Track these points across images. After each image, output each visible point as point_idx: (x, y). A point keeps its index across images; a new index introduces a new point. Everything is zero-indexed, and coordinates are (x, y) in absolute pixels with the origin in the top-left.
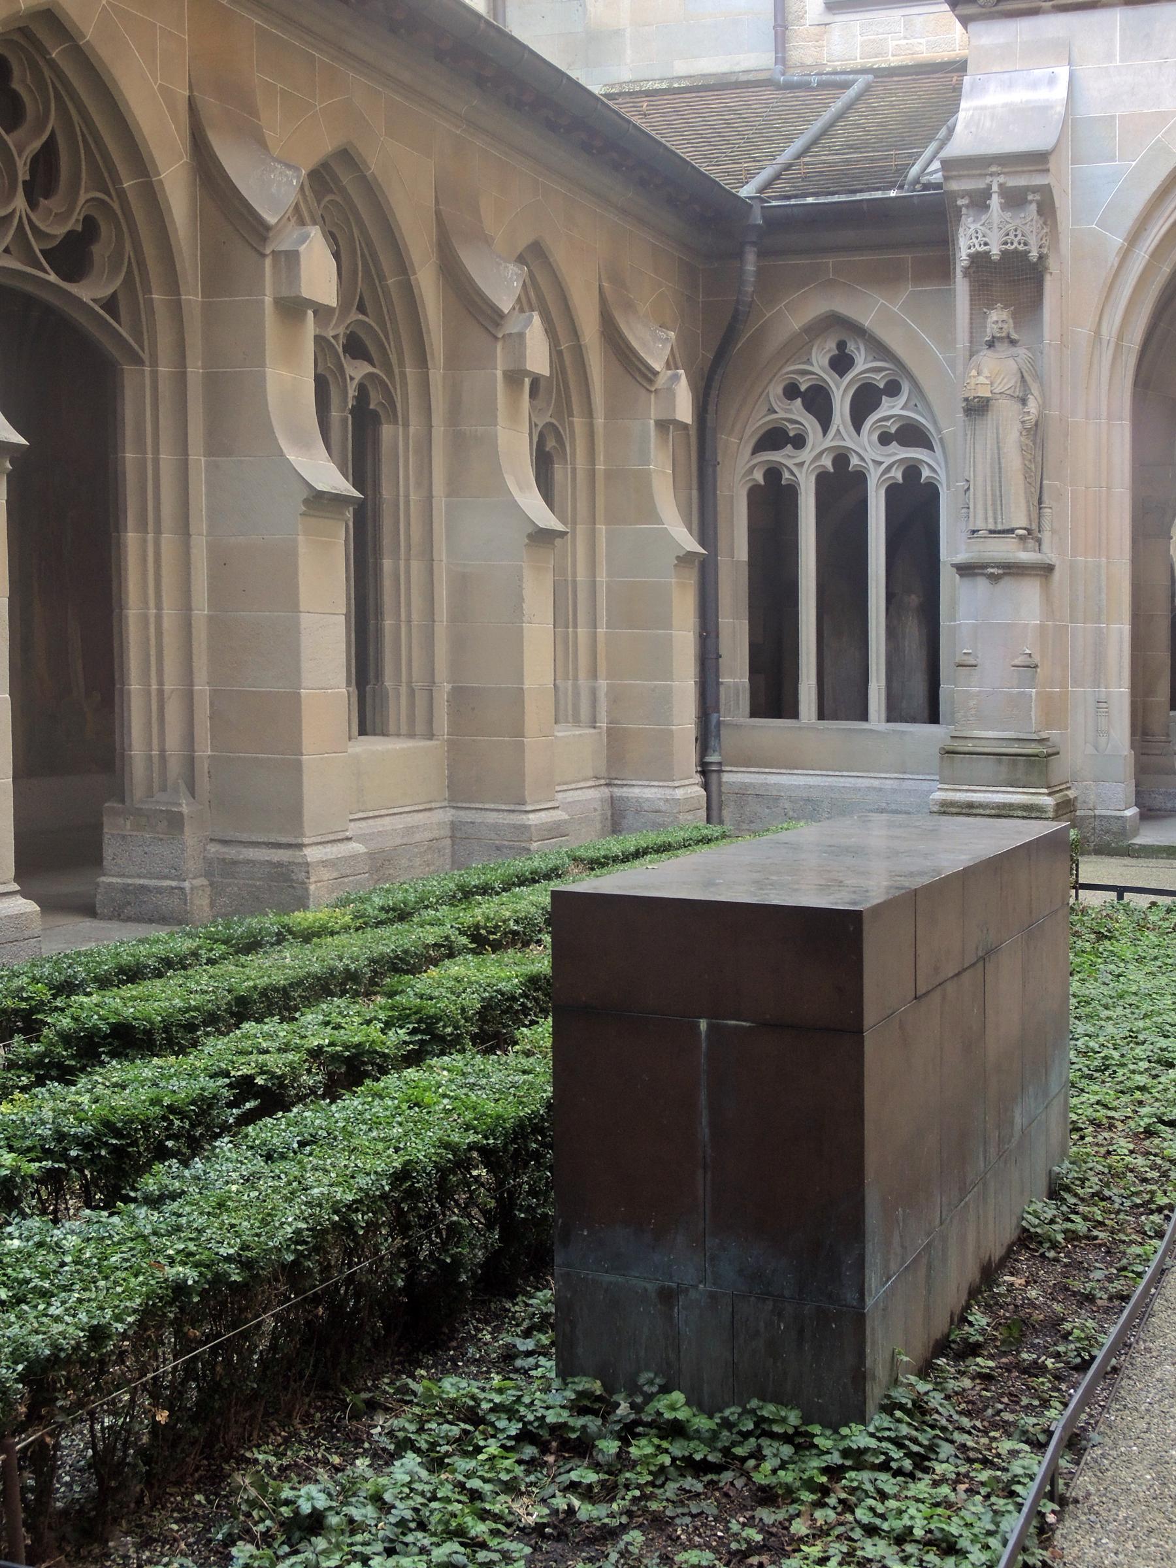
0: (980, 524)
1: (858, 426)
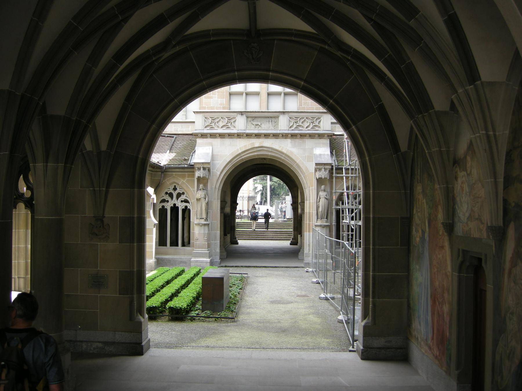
0: (198, 217)
1: (177, 198)
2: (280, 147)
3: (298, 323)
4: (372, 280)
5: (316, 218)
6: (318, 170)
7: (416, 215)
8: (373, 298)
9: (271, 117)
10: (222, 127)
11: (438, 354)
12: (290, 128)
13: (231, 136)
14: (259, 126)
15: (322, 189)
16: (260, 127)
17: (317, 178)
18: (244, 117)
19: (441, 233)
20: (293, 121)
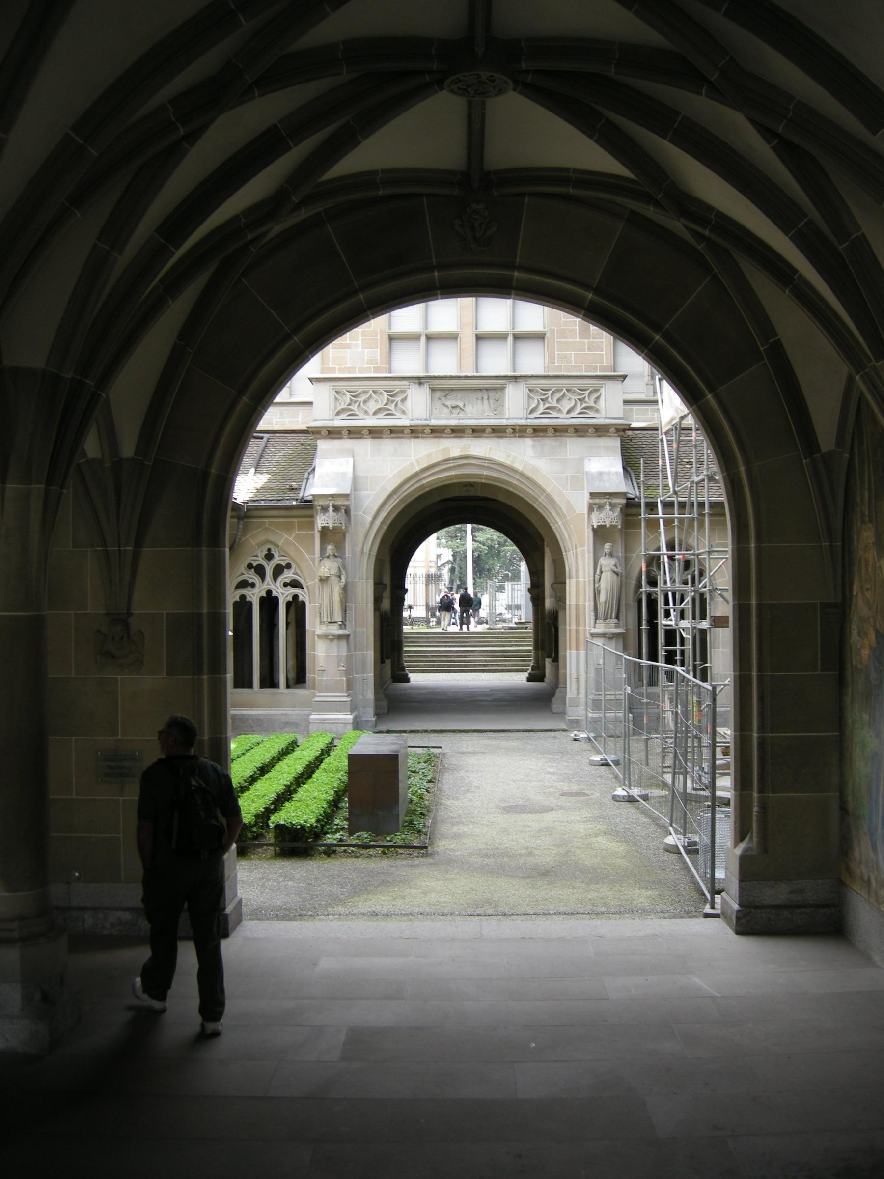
0: (325, 620)
2: (509, 456)
3: (574, 855)
4: (759, 750)
5: (593, 617)
6: (595, 509)
7: (860, 596)
8: (761, 791)
9: (487, 389)
10: (375, 413)
12: (532, 412)
13: (395, 432)
14: (461, 409)
15: (606, 550)
16: (461, 411)
17: (593, 526)
18: (425, 390)
20: (537, 397)
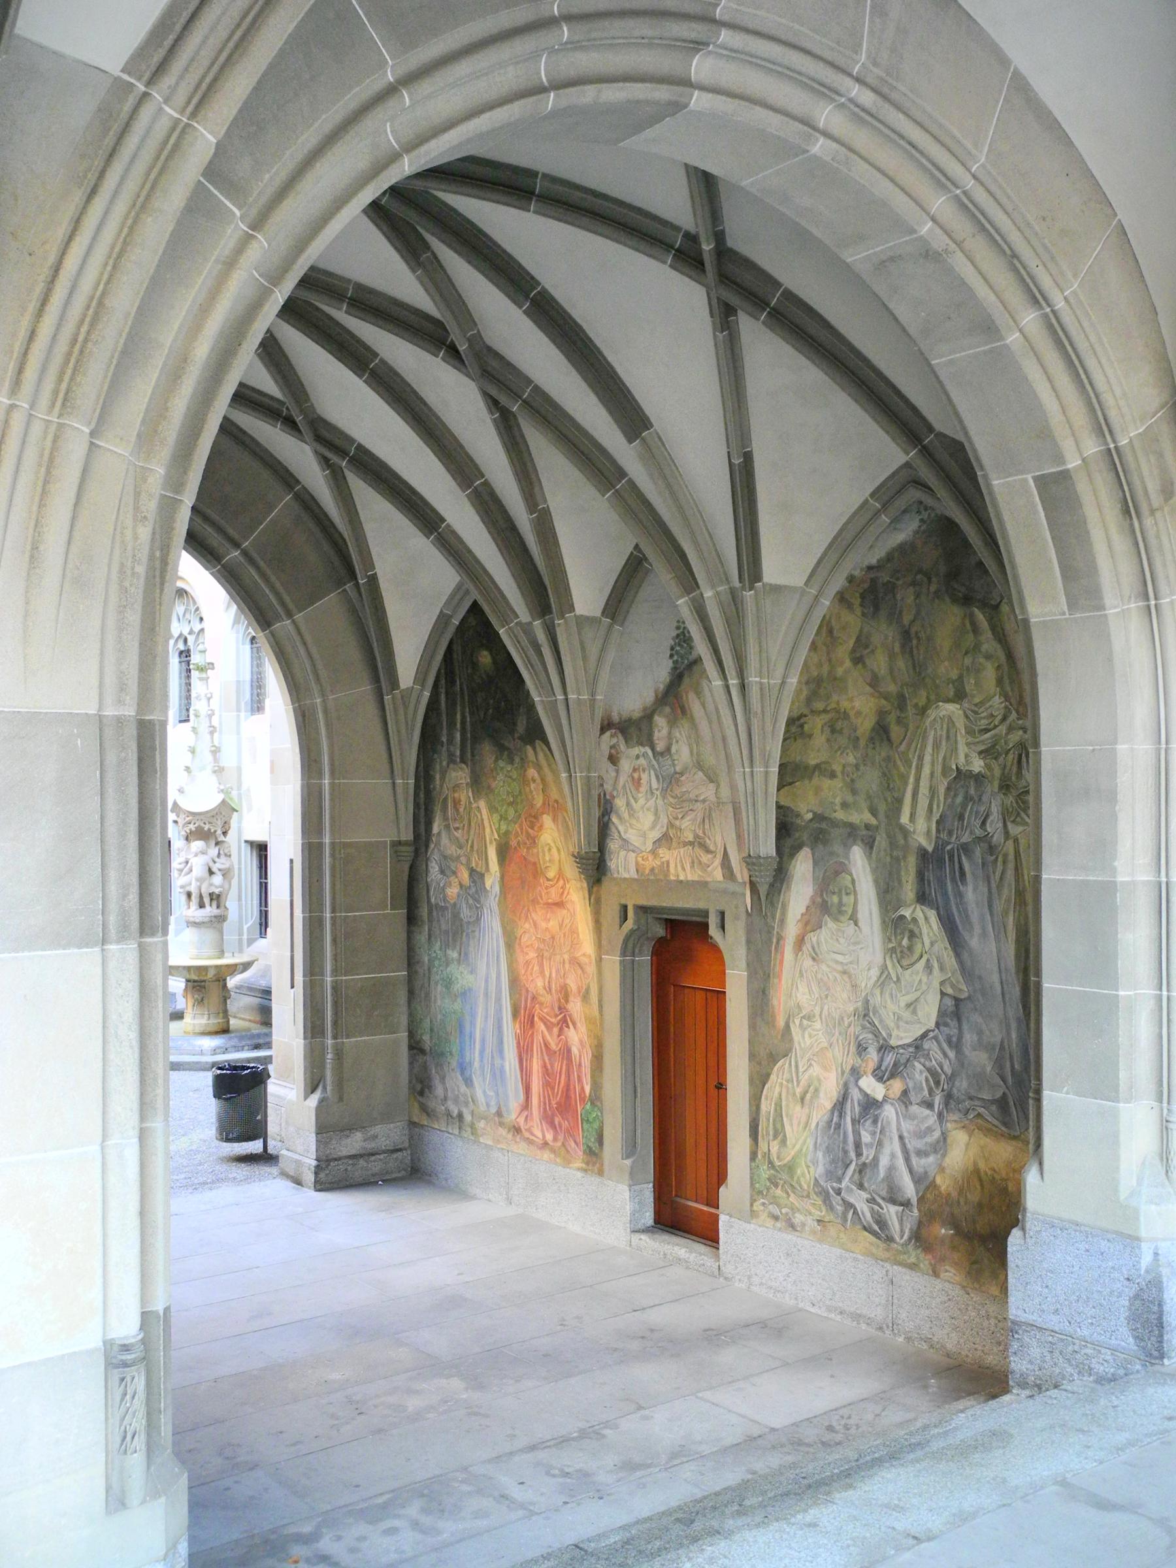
7: (444, 835)
8: (335, 1037)
11: (549, 1137)
19: (551, 874)
